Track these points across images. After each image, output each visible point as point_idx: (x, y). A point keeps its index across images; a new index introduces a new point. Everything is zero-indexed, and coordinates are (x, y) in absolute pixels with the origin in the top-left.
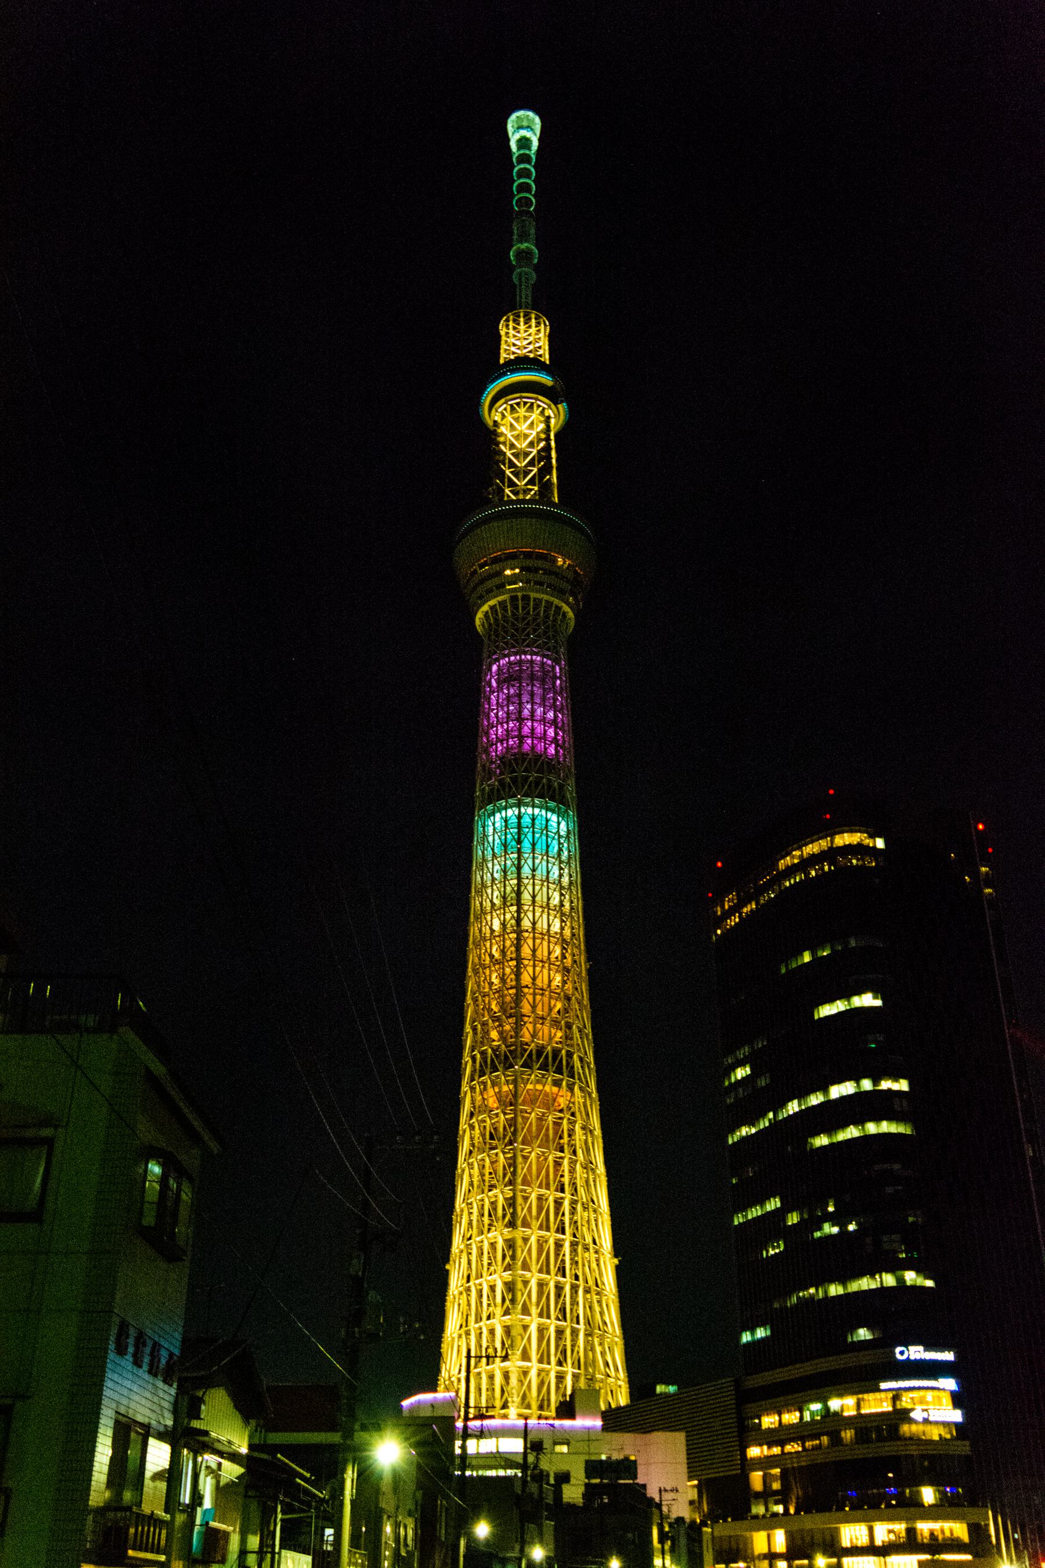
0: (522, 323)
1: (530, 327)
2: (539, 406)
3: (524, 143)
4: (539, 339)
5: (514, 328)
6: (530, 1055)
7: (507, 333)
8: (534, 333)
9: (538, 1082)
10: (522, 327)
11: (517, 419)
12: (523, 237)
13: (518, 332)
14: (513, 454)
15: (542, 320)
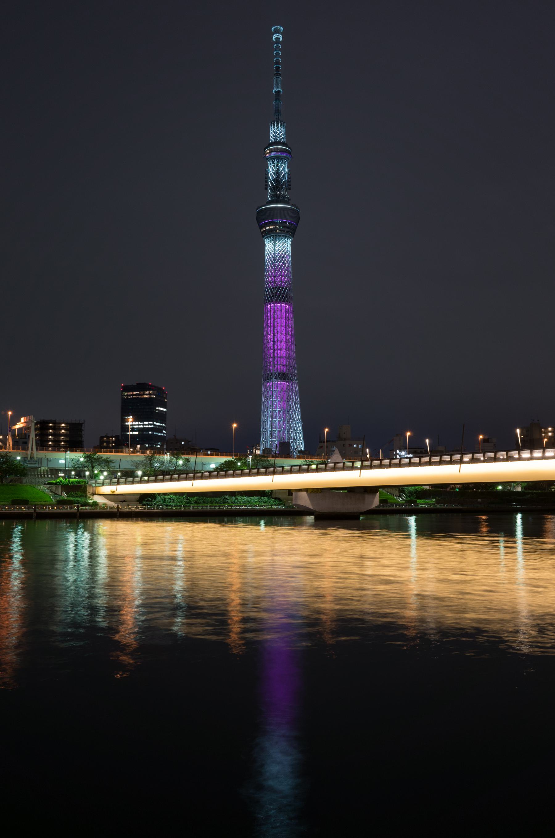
0: (276, 126)
1: (278, 127)
2: (281, 160)
3: (277, 39)
4: (282, 131)
5: (274, 128)
6: (277, 375)
7: (271, 129)
8: (280, 129)
9: (279, 381)
10: (276, 127)
11: (274, 166)
12: (277, 87)
13: (275, 129)
14: (272, 180)
15: (283, 123)
